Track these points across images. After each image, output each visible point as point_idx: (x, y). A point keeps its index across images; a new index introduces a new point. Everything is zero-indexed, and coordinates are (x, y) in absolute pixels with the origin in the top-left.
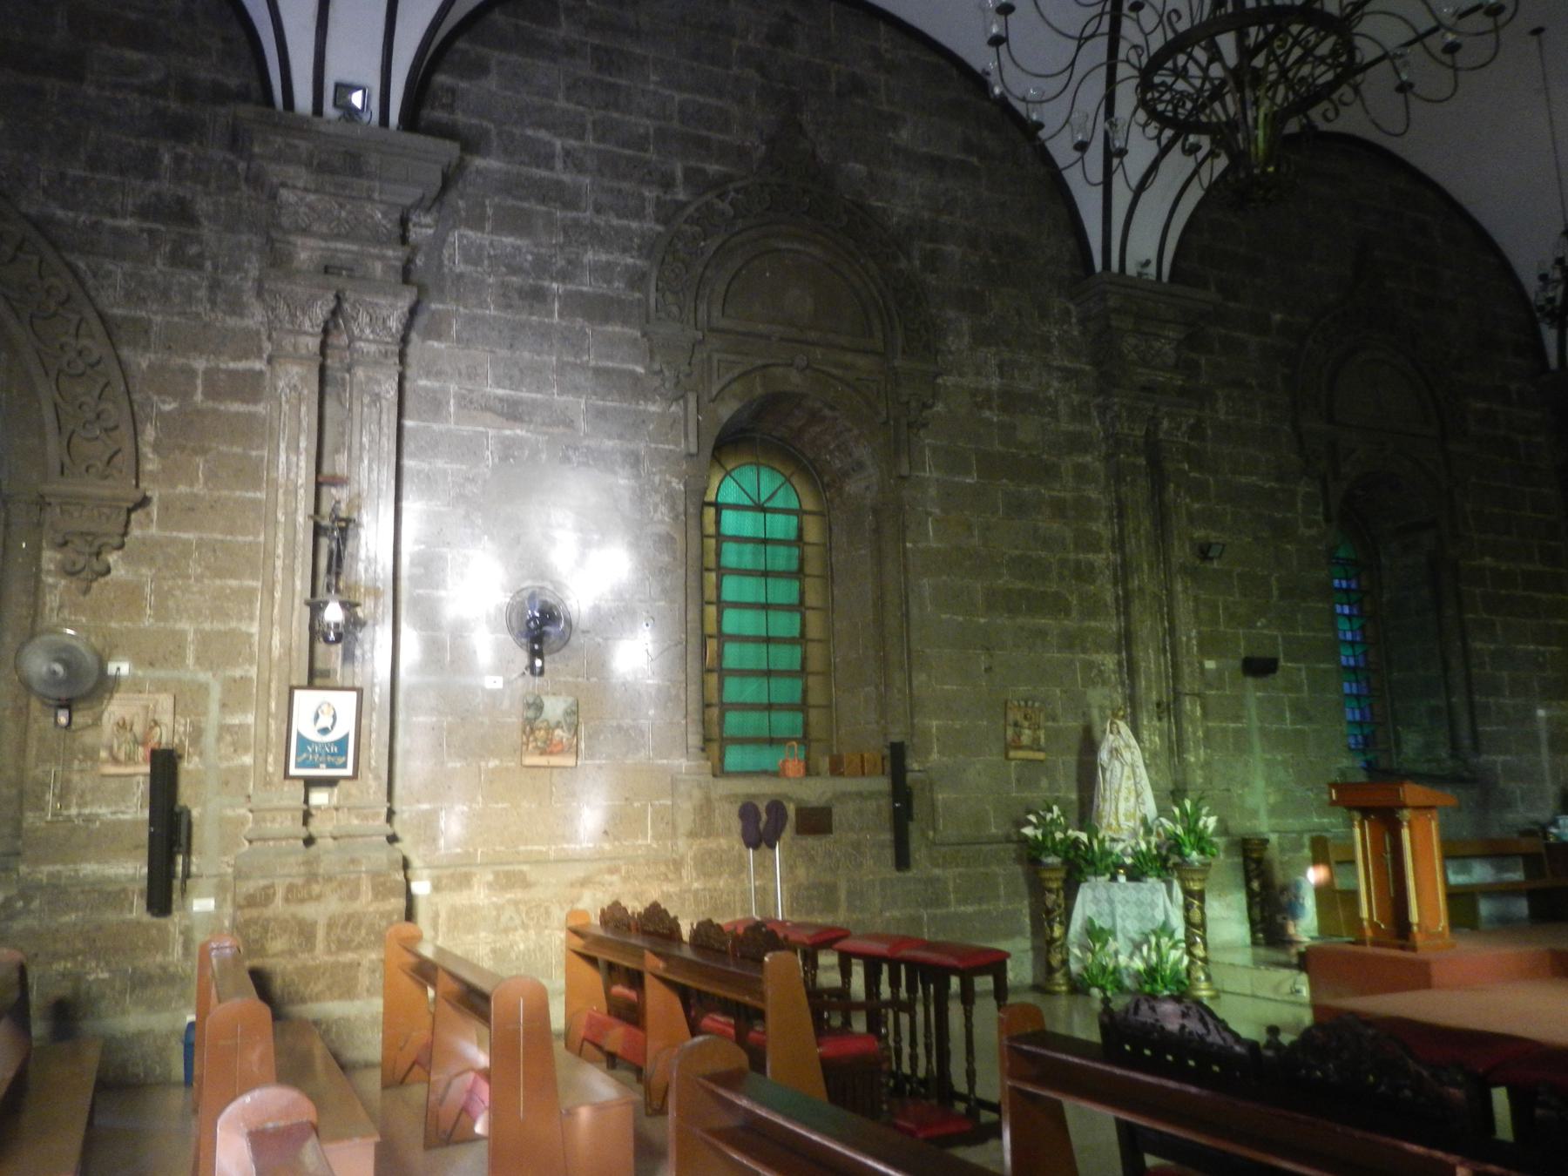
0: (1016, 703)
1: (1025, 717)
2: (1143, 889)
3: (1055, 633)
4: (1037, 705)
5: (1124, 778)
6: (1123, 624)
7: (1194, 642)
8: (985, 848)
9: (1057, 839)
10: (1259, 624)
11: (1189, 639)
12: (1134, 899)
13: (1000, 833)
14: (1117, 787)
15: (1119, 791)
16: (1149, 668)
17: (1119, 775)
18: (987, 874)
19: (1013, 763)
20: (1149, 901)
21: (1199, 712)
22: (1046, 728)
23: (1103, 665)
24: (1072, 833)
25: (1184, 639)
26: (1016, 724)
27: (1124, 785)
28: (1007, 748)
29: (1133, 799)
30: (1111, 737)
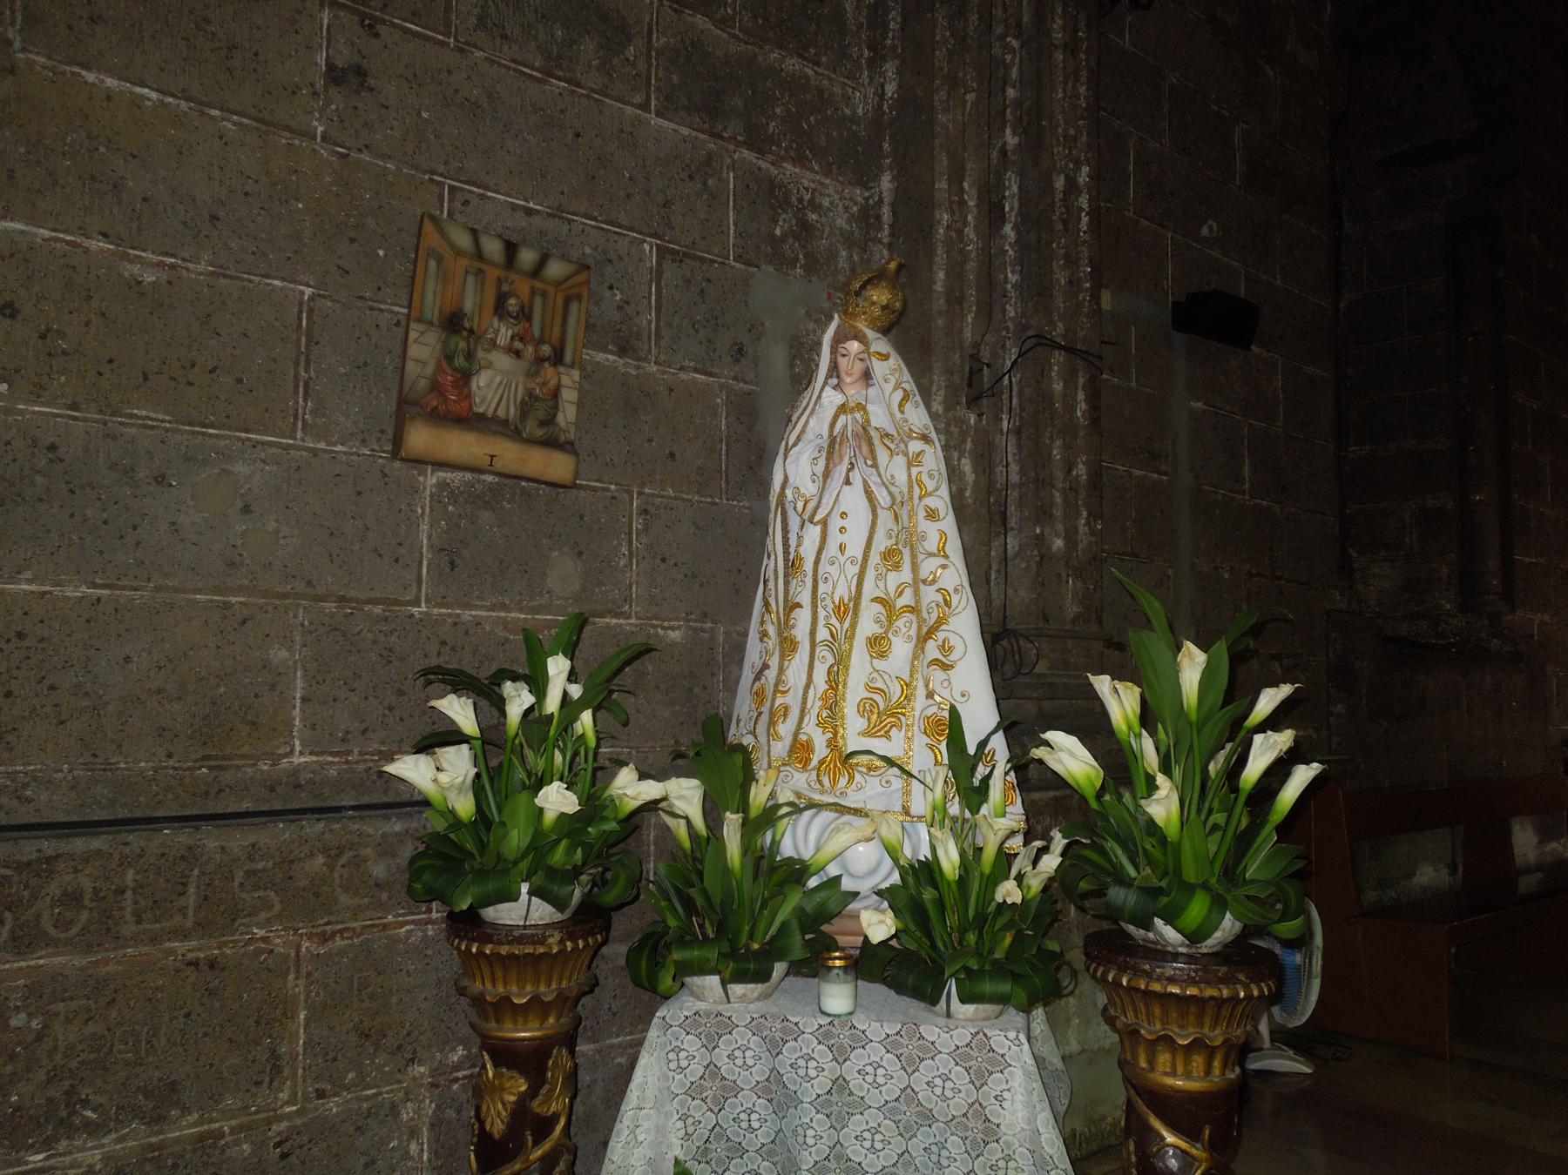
0: (463, 240)
1: (500, 308)
2: (932, 1051)
3: (659, 42)
4: (555, 269)
5: (875, 558)
6: (890, 89)
7: (1083, 201)
8: (211, 841)
9: (550, 817)
10: (1205, 231)
11: (1072, 187)
12: (891, 1090)
13: (334, 767)
14: (843, 591)
15: (849, 609)
16: (960, 232)
17: (856, 549)
18: (212, 964)
19: (431, 479)
20: (958, 1106)
21: (1081, 408)
22: (589, 374)
23: (814, 206)
24: (630, 788)
25: (1060, 183)
26: (453, 322)
27: (869, 590)
28: (406, 408)
29: (901, 649)
30: (832, 398)
